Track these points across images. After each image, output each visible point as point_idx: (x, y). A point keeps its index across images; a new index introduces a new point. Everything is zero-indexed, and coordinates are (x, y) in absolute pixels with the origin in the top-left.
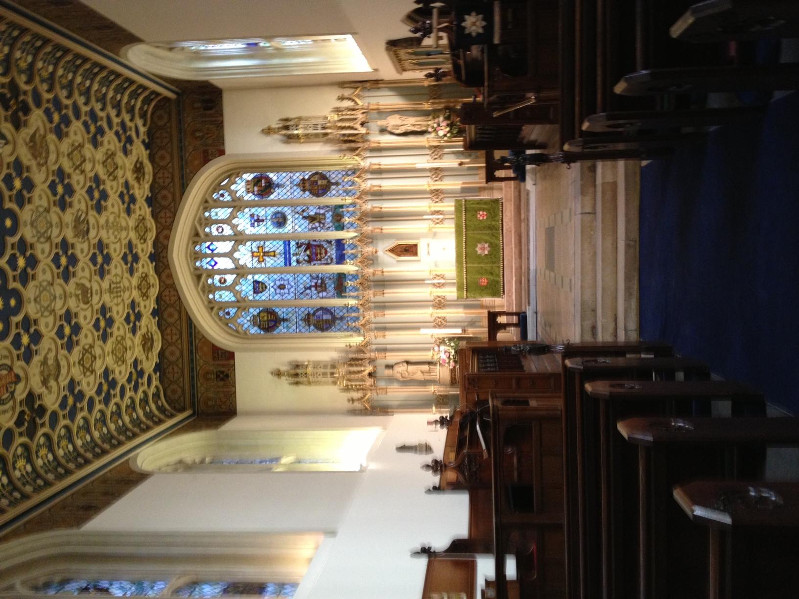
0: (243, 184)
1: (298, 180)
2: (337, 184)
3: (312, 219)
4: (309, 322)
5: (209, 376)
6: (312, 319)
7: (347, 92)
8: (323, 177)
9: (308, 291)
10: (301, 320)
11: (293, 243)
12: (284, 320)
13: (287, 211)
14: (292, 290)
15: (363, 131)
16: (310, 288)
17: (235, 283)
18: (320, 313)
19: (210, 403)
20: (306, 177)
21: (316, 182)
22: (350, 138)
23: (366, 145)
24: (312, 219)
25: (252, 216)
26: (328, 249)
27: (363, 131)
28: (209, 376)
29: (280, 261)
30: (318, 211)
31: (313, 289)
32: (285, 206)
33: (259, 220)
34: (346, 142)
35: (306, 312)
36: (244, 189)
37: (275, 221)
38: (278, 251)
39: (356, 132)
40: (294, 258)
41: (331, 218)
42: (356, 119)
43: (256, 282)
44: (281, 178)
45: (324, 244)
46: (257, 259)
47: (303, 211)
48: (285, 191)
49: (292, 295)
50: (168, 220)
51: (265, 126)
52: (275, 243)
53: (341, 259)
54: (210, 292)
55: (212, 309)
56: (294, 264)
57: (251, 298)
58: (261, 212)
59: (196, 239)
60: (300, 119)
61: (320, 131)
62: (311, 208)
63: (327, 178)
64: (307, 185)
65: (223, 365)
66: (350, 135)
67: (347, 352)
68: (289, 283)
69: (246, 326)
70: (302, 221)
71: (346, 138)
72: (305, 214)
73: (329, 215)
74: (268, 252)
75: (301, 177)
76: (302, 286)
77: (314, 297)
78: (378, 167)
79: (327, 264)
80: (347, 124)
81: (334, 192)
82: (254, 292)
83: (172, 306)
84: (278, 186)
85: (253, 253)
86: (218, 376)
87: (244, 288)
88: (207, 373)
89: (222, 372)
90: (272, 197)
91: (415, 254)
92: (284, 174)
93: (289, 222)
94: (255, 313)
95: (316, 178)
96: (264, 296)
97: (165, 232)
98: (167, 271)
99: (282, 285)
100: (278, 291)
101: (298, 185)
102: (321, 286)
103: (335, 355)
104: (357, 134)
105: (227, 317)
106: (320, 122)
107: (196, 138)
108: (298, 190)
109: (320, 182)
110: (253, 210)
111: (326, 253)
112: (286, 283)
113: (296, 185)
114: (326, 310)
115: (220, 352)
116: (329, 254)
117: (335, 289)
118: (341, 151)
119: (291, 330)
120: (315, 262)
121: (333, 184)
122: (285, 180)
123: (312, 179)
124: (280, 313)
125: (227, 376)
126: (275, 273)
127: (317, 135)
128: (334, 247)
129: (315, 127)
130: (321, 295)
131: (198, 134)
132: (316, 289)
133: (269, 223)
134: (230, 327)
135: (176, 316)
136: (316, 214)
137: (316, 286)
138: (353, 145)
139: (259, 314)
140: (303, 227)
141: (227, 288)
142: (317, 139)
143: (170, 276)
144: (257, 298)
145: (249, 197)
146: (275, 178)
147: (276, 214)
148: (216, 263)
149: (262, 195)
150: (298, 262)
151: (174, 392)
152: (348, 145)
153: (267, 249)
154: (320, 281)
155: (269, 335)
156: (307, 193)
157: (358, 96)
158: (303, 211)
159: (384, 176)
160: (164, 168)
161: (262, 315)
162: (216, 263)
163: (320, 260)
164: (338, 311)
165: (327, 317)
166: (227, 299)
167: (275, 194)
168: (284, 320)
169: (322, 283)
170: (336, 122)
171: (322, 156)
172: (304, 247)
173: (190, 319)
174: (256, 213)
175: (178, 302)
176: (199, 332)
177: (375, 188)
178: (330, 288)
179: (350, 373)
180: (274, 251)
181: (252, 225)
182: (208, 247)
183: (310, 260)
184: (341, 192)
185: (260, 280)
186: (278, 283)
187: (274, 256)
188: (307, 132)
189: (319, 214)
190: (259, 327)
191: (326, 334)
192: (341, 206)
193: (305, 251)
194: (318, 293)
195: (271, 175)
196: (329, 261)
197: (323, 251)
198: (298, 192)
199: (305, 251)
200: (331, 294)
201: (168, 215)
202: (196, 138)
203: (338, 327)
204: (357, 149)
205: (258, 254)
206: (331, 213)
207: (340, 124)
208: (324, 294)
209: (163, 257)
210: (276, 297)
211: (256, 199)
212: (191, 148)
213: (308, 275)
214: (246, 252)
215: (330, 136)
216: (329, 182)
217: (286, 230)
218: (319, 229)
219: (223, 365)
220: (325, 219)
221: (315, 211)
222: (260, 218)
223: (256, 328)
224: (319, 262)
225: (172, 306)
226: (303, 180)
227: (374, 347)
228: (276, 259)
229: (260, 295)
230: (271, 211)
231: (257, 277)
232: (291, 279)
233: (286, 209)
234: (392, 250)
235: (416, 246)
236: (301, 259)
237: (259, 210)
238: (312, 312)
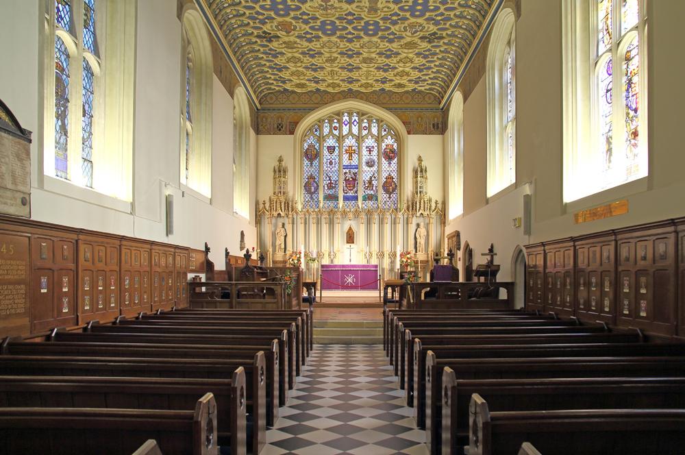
0: (391, 143)
5: (280, 119)
7: (440, 206)
11: (357, 171)
13: (375, 168)
16: (330, 180)
19: (264, 119)
23: (410, 216)
24: (370, 182)
25: (373, 147)
27: (418, 214)
28: (280, 119)
33: (370, 151)
36: (388, 143)
43: (334, 148)
47: (375, 177)
56: (344, 171)
59: (361, 114)
60: (426, 178)
61: (419, 190)
62: (376, 182)
65: (286, 128)
66: (416, 206)
72: (373, 178)
79: (344, 190)
80: (422, 206)
84: (390, 163)
90: (383, 159)
93: (369, 169)
96: (326, 152)
97: (365, 97)
100: (329, 161)
107: (418, 118)
114: (317, 188)
118: (408, 201)
121: (390, 195)
127: (417, 188)
131: (420, 119)
137: (331, 183)
138: (411, 208)
143: (339, 99)
146: (394, 161)
148: (346, 125)
150: (346, 173)
151: (271, 98)
157: (437, 212)
158: (375, 177)
162: (346, 125)
164: (316, 196)
168: (311, 164)
171: (406, 190)
176: (306, 115)
183: (345, 180)
186: (333, 161)
192: (377, 200)
195: (396, 159)
207: (422, 201)
217: (364, 167)
227: (295, 217)
230: (375, 158)
231: (337, 148)
234: (350, 228)
237: (376, 152)
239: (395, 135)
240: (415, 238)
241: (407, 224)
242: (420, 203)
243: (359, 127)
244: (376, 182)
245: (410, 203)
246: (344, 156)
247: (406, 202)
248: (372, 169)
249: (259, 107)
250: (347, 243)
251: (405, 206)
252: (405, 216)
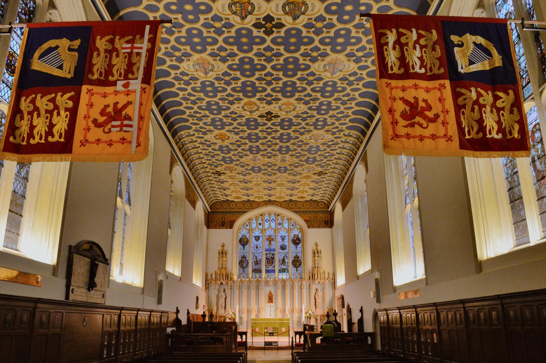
1: (298, 255)
3: (283, 260)
6: (244, 259)
7: (331, 276)
8: (300, 265)
9: (255, 258)
11: (274, 252)
12: (244, 248)
16: (256, 258)
19: (213, 219)
24: (283, 260)
25: (285, 237)
33: (283, 239)
34: (312, 275)
40: (268, 252)
51: (318, 244)
53: (267, 271)
54: (256, 219)
55: (249, 220)
56: (266, 252)
59: (276, 215)
60: (321, 257)
62: (288, 260)
65: (227, 224)
72: (285, 257)
73: (285, 267)
81: (294, 269)
83: (251, 206)
84: (296, 247)
86: (223, 222)
89: (225, 224)
90: (292, 245)
93: (282, 251)
96: (254, 240)
97: (279, 204)
109: (297, 264)
110: (287, 237)
111: (270, 265)
112: (259, 249)
114: (247, 265)
118: (309, 273)
125: (223, 226)
126: (262, 245)
127: (315, 264)
129: (318, 264)
135: (247, 207)
137: (257, 261)
138: (311, 278)
141: (257, 226)
143: (262, 206)
145: (292, 236)
146: (299, 246)
150: (267, 254)
151: (218, 205)
152: (311, 276)
153: (272, 242)
155: (238, 241)
159: (299, 290)
160: (303, 205)
161: (246, 239)
164: (247, 269)
168: (244, 248)
172: (272, 257)
179: (223, 275)
181: (281, 237)
182: (273, 219)
183: (267, 258)
186: (258, 246)
190: (241, 238)
191: (238, 264)
192: (288, 272)
195: (300, 245)
198: (294, 255)
201: (286, 206)
203: (240, 269)
207: (319, 273)
208: (254, 264)
212: (310, 215)
215: (314, 269)
216: (298, 267)
219: (227, 224)
223: (241, 236)
225: (251, 206)
226: (298, 257)
231: (261, 237)
234: (270, 293)
239: (300, 229)
240: (315, 299)
241: (309, 288)
242: (317, 274)
243: (275, 223)
245: (311, 275)
246: (266, 242)
247: (308, 273)
248: (284, 251)
249: (209, 210)
251: (308, 276)
252: (308, 284)
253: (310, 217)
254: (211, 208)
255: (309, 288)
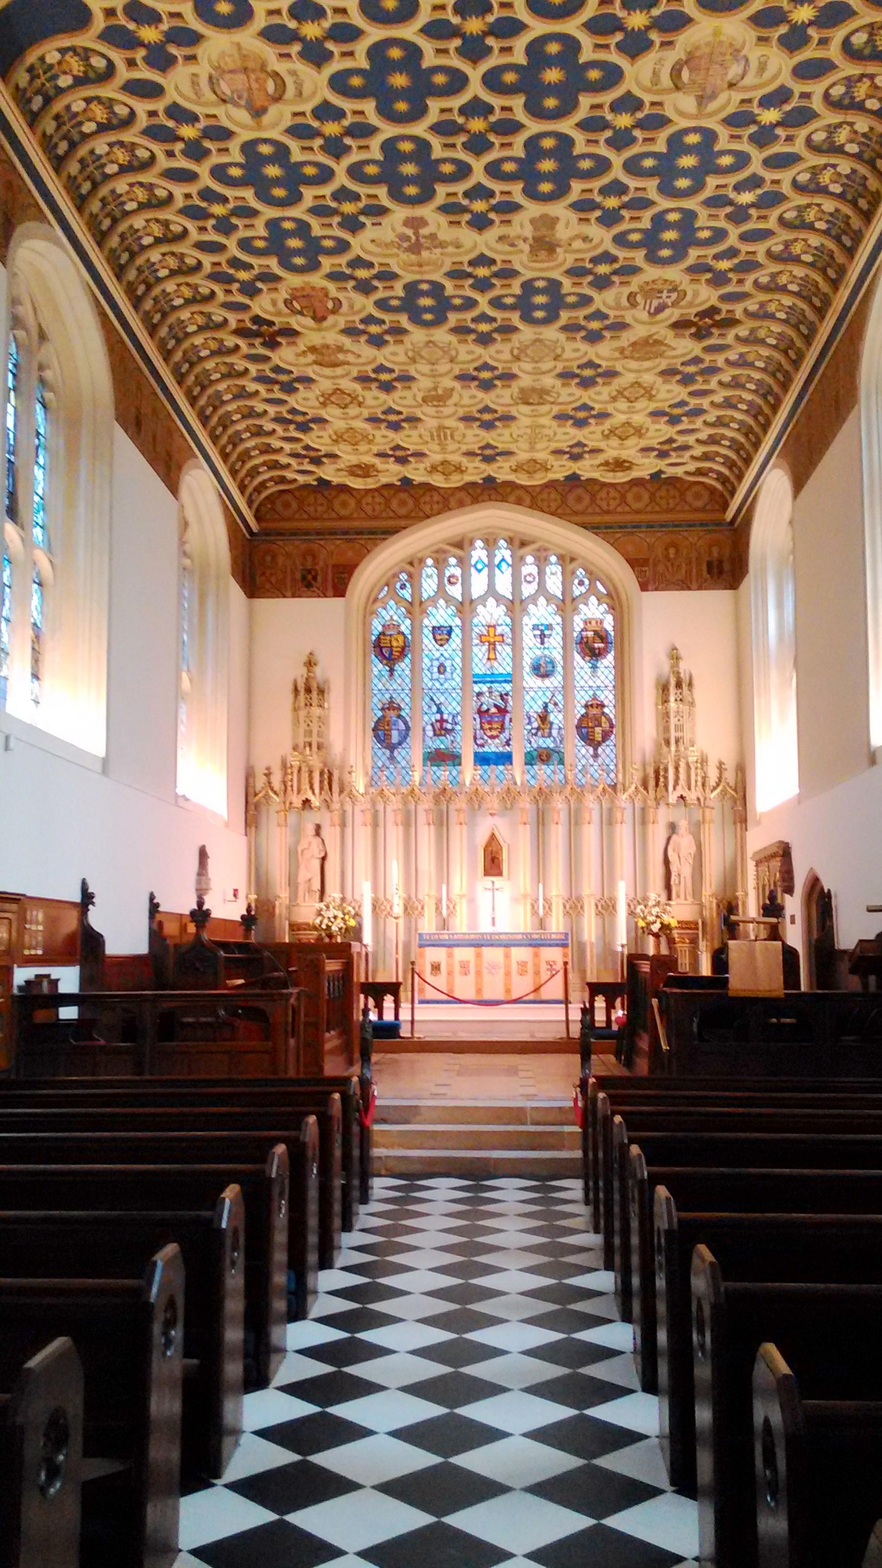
0: (598, 615)
1: (602, 698)
2: (596, 756)
3: (544, 718)
4: (389, 709)
6: (392, 714)
7: (730, 776)
9: (434, 709)
10: (391, 698)
11: (508, 687)
12: (392, 671)
13: (556, 680)
14: (437, 685)
15: (673, 798)
17: (449, 599)
18: (402, 726)
19: (268, 558)
20: (606, 710)
21: (600, 725)
22: (662, 779)
23: (651, 803)
24: (544, 718)
25: (549, 627)
26: (497, 741)
27: (673, 798)
29: (479, 667)
30: (555, 726)
31: (438, 716)
32: (565, 677)
33: (542, 636)
34: (657, 773)
35: (402, 706)
36: (590, 616)
37: (542, 662)
38: (496, 664)
39: (671, 788)
40: (484, 688)
41: (544, 746)
42: (689, 789)
44: (606, 672)
45: (506, 734)
46: (485, 632)
47: (556, 704)
48: (586, 677)
49: (430, 684)
50: (546, 504)
51: (682, 652)
52: (509, 660)
56: (477, 688)
57: (426, 622)
58: (555, 641)
59: (517, 542)
60: (692, 704)
63: (604, 740)
64: (595, 711)
65: (325, 580)
66: (666, 778)
67: (341, 768)
68: (446, 679)
69: (384, 613)
70: (540, 703)
71: (662, 773)
72: (551, 707)
73: (549, 743)
74: (494, 649)
75: (606, 702)
76: (442, 699)
77: (426, 718)
78: (619, 820)
79: (475, 738)
82: (434, 628)
84: (594, 667)
85: (494, 627)
87: (441, 611)
88: (314, 557)
89: (315, 578)
90: (577, 657)
91: (487, 873)
92: (611, 677)
94: (403, 628)
95: (605, 725)
96: (428, 641)
97: (528, 500)
98: (468, 500)
99: (445, 670)
100: (436, 663)
101: (595, 697)
102: (442, 728)
103: (336, 747)
104: (667, 790)
105: (398, 586)
106: (687, 736)
107: (666, 549)
108: (587, 698)
109: (598, 730)
110: (558, 629)
111: (492, 737)
112: (448, 675)
113: (595, 694)
115: (346, 575)
116: (490, 741)
117: (438, 750)
118: (644, 765)
119: (376, 681)
120: (478, 720)
122: (603, 677)
123: (603, 719)
124: (403, 665)
125: (309, 586)
126: (463, 659)
127: (667, 729)
128: (501, 749)
130: (429, 728)
132: (437, 721)
133: (539, 653)
134: (383, 589)
135: (403, 511)
136: (551, 723)
137: (442, 721)
138: (652, 783)
139: (403, 634)
140: (532, 703)
141: (441, 585)
142: (661, 728)
143: (461, 504)
144: (426, 631)
145: (578, 623)
147: (552, 662)
148: (479, 571)
149: (581, 643)
150: (479, 694)
151: (287, 505)
152: (652, 775)
153: (499, 647)
154: (449, 726)
156: (583, 711)
157: (724, 793)
158: (556, 704)
160: (623, 500)
161: (401, 638)
162: (479, 571)
163: (482, 728)
165: (395, 737)
166: (425, 585)
167: (582, 663)
168: (392, 671)
169: (446, 730)
170: (686, 758)
173: (397, 532)
174: (554, 633)
175: (421, 514)
176: (376, 545)
177: (587, 816)
178: (438, 742)
179: (311, 772)
180: (496, 659)
181: (535, 627)
182: (503, 560)
184: (584, 761)
185: (453, 635)
186: (448, 664)
187: (489, 659)
188: (672, 715)
189: (550, 729)
190: (382, 634)
191: (370, 733)
192: (561, 762)
193: (496, 706)
194: (432, 725)
196: (479, 742)
197: (494, 733)
198: (582, 697)
199: (496, 706)
200: (430, 744)
202: (666, 549)
203: (379, 753)
204: (646, 788)
205: (492, 634)
206: (552, 746)
207: (682, 764)
208: (430, 733)
209: (490, 496)
210: (426, 660)
211: (575, 634)
213: (459, 709)
214: (496, 616)
215: (665, 749)
216: (599, 744)
217: (526, 677)
218: (529, 727)
219: (325, 580)
220: (543, 736)
221: (556, 721)
222: (546, 640)
223: (380, 629)
224: (478, 726)
228: (485, 661)
229: (431, 636)
230: (557, 655)
231: (457, 631)
232: (454, 684)
233: (560, 678)
234: (493, 837)
235: (500, 874)
236: (483, 699)
237: (559, 639)
238: (403, 713)
242: (677, 768)
244: (560, 716)
250: (487, 873)
251: (637, 777)
252: (638, 805)
253: (650, 547)
254: (258, 517)
255: (644, 822)
